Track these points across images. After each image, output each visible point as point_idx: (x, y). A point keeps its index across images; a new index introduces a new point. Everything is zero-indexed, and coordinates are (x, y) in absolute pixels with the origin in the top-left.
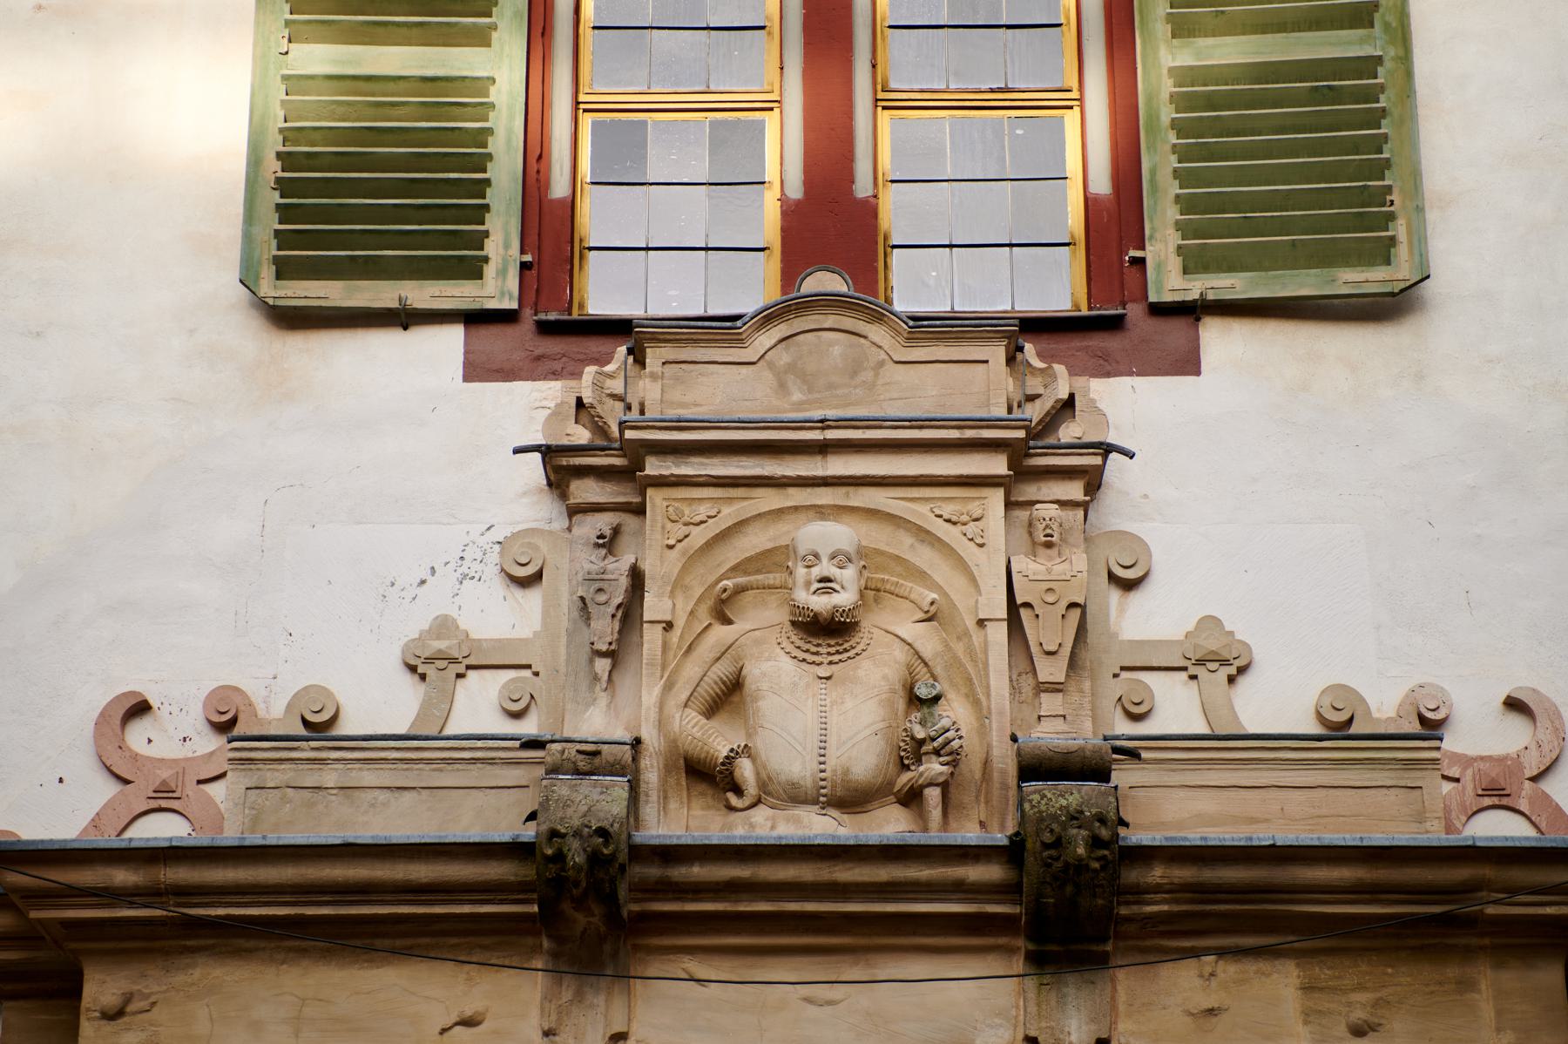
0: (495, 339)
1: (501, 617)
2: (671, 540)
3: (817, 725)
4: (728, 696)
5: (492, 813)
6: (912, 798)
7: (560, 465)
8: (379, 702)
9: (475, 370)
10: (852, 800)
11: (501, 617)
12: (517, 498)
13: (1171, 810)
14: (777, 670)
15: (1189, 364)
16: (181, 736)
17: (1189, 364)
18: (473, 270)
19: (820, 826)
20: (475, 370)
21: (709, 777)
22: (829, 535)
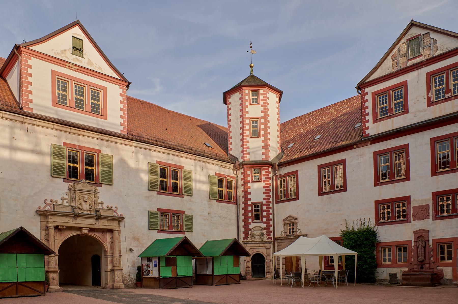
0: (66, 180)
1: (66, 197)
2: (78, 195)
3: (86, 207)
4: (81, 204)
5: (69, 210)
6: (90, 211)
7: (70, 189)
8: (60, 202)
9: (64, 182)
10: (87, 211)
11: (66, 197)
12: (67, 191)
13: (103, 213)
14: (83, 203)
15: (101, 187)
16: (48, 202)
17: (101, 187)
18: (64, 176)
19: (86, 212)
20: (64, 182)
21: (80, 209)
22: (86, 196)
